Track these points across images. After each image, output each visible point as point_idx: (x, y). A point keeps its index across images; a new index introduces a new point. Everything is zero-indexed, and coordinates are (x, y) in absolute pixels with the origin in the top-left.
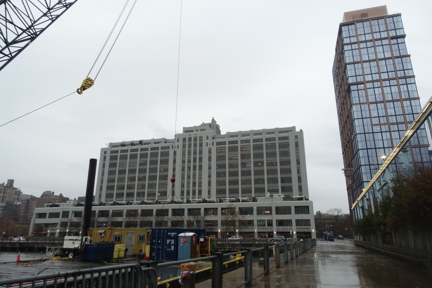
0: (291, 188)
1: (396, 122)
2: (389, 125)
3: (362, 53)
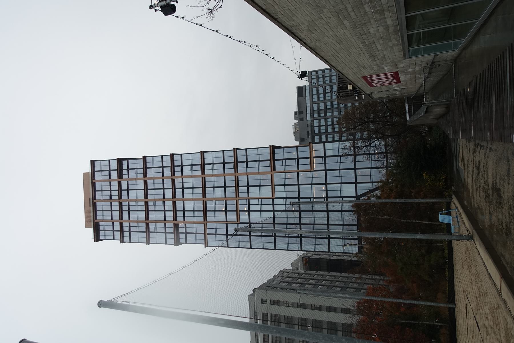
0: (346, 325)
1: (234, 188)
2: (239, 199)
3: (136, 218)
